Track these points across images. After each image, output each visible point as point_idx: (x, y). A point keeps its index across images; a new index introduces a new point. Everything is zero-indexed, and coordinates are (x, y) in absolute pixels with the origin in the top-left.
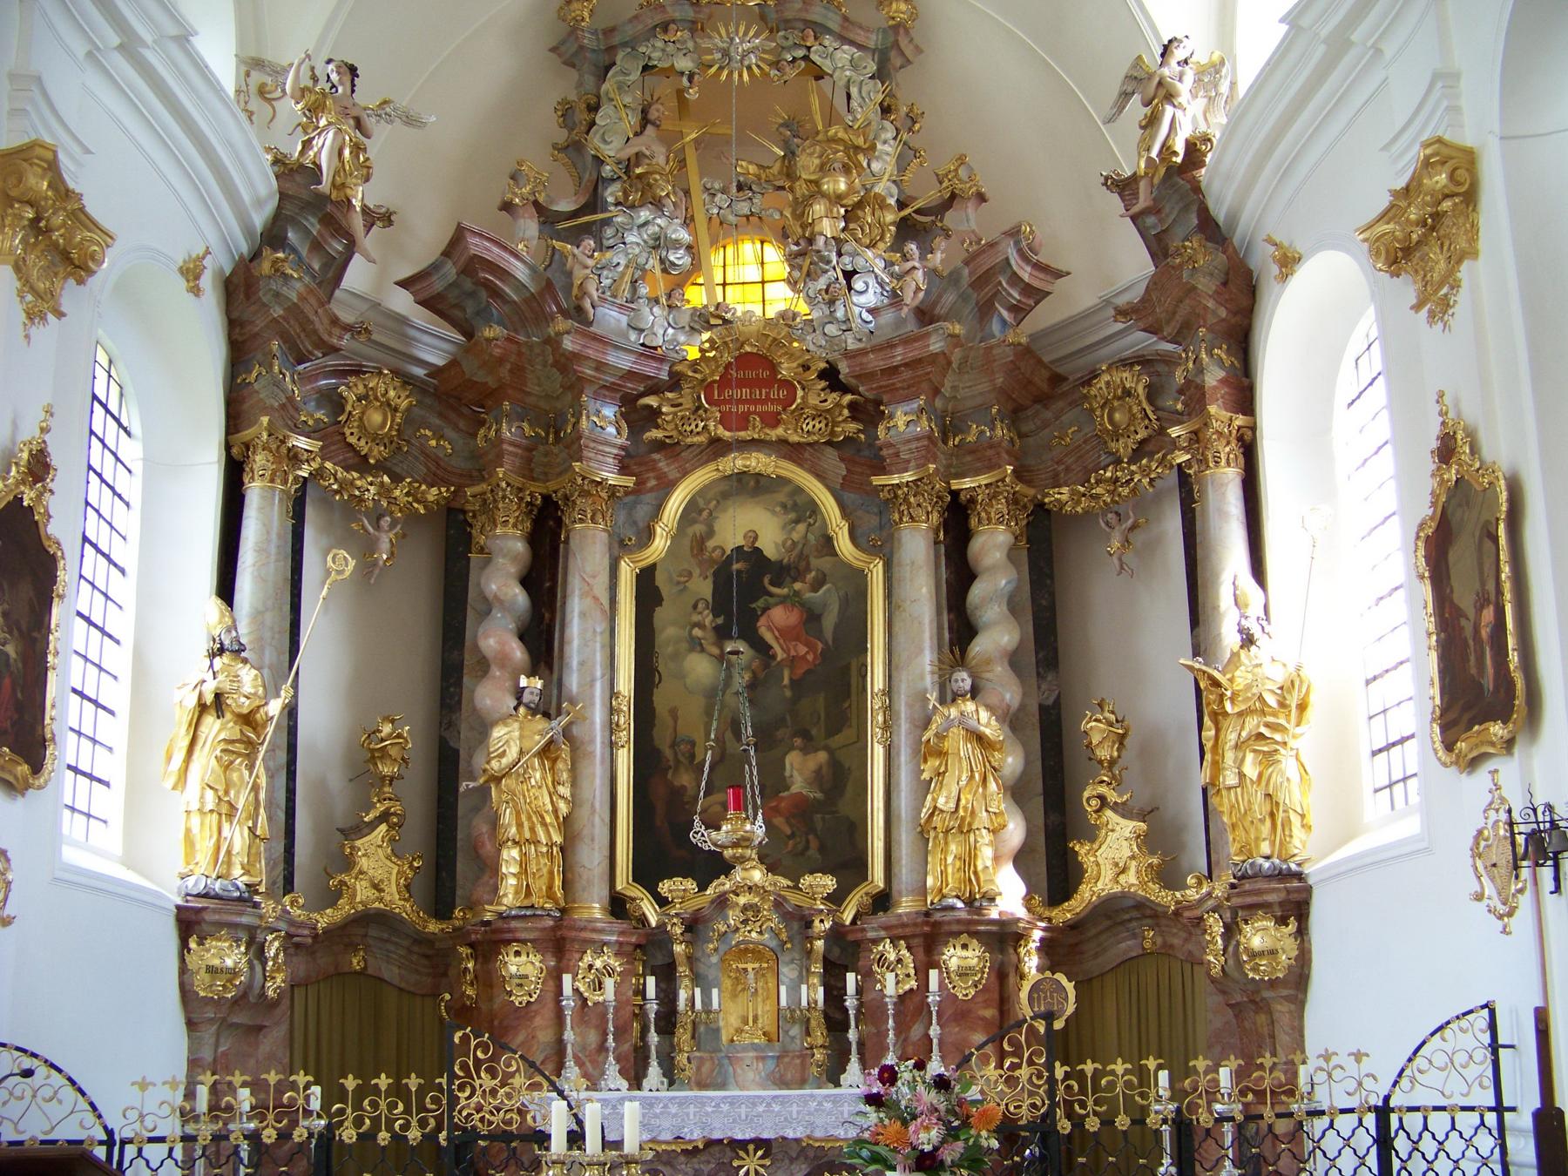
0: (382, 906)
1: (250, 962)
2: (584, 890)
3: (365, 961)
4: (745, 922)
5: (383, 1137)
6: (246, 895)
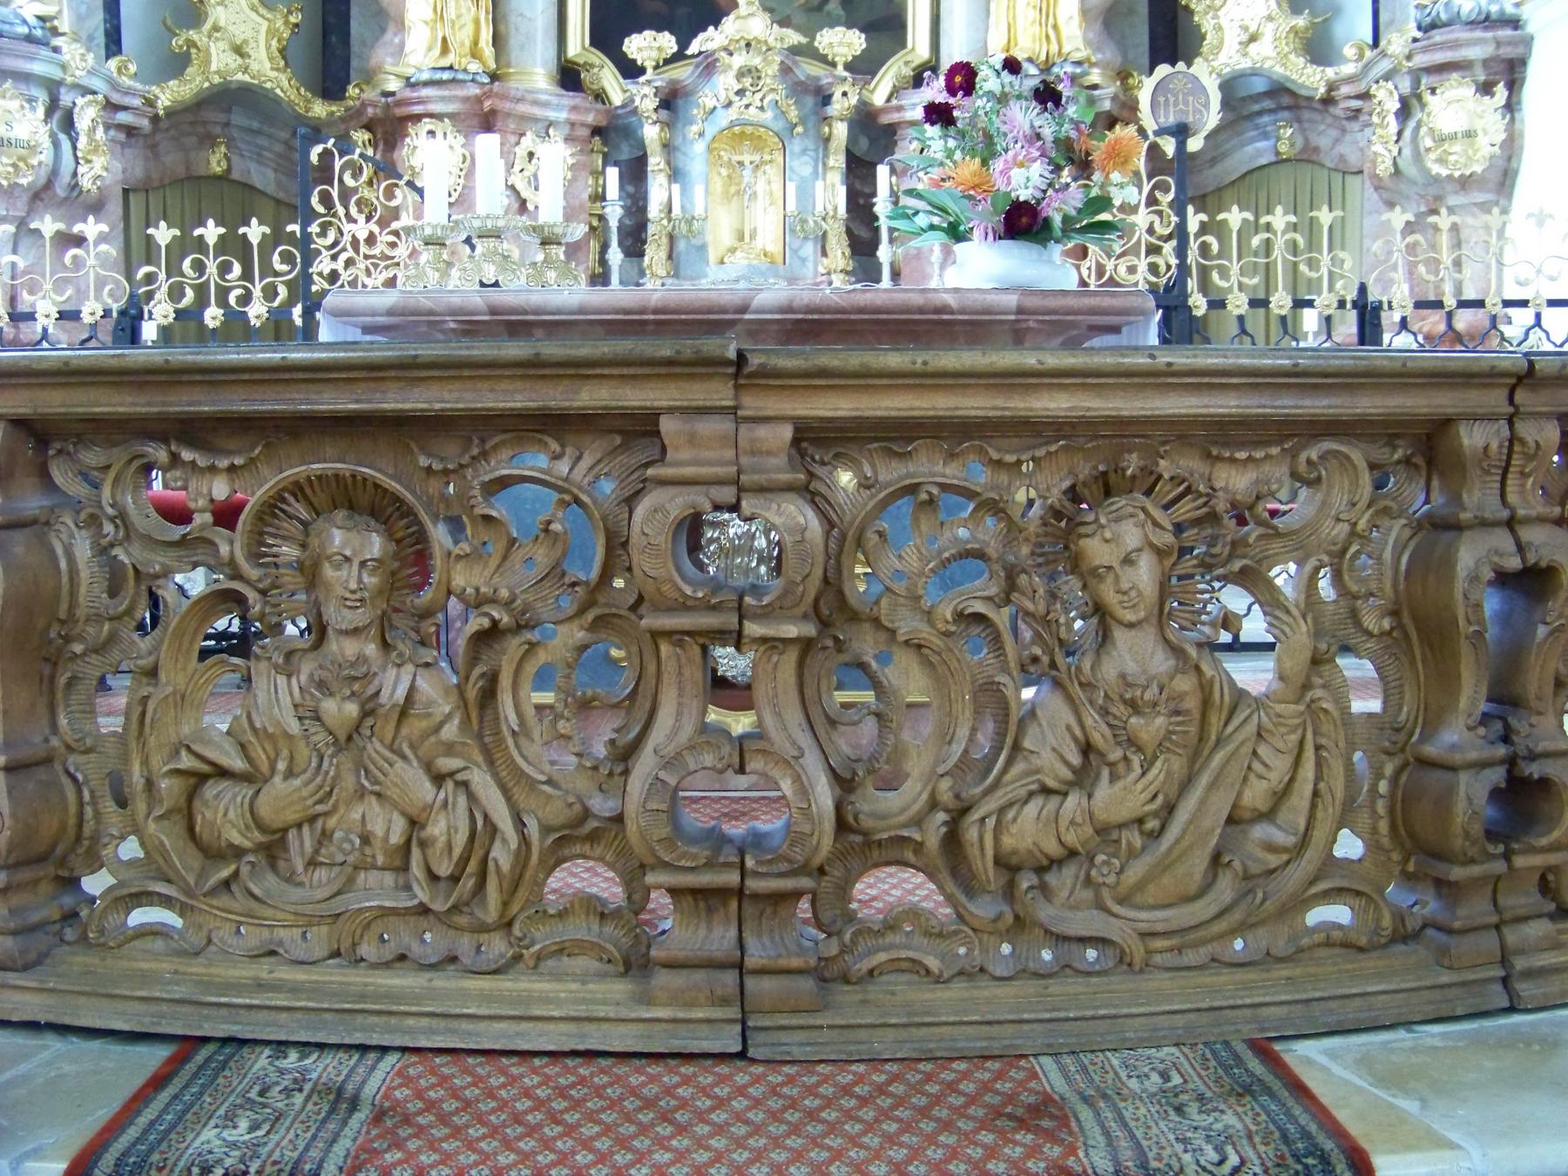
0: (247, 78)
1: (53, 136)
2: (522, 48)
3: (228, 160)
4: (741, 93)
5: (213, 316)
6: (38, 33)
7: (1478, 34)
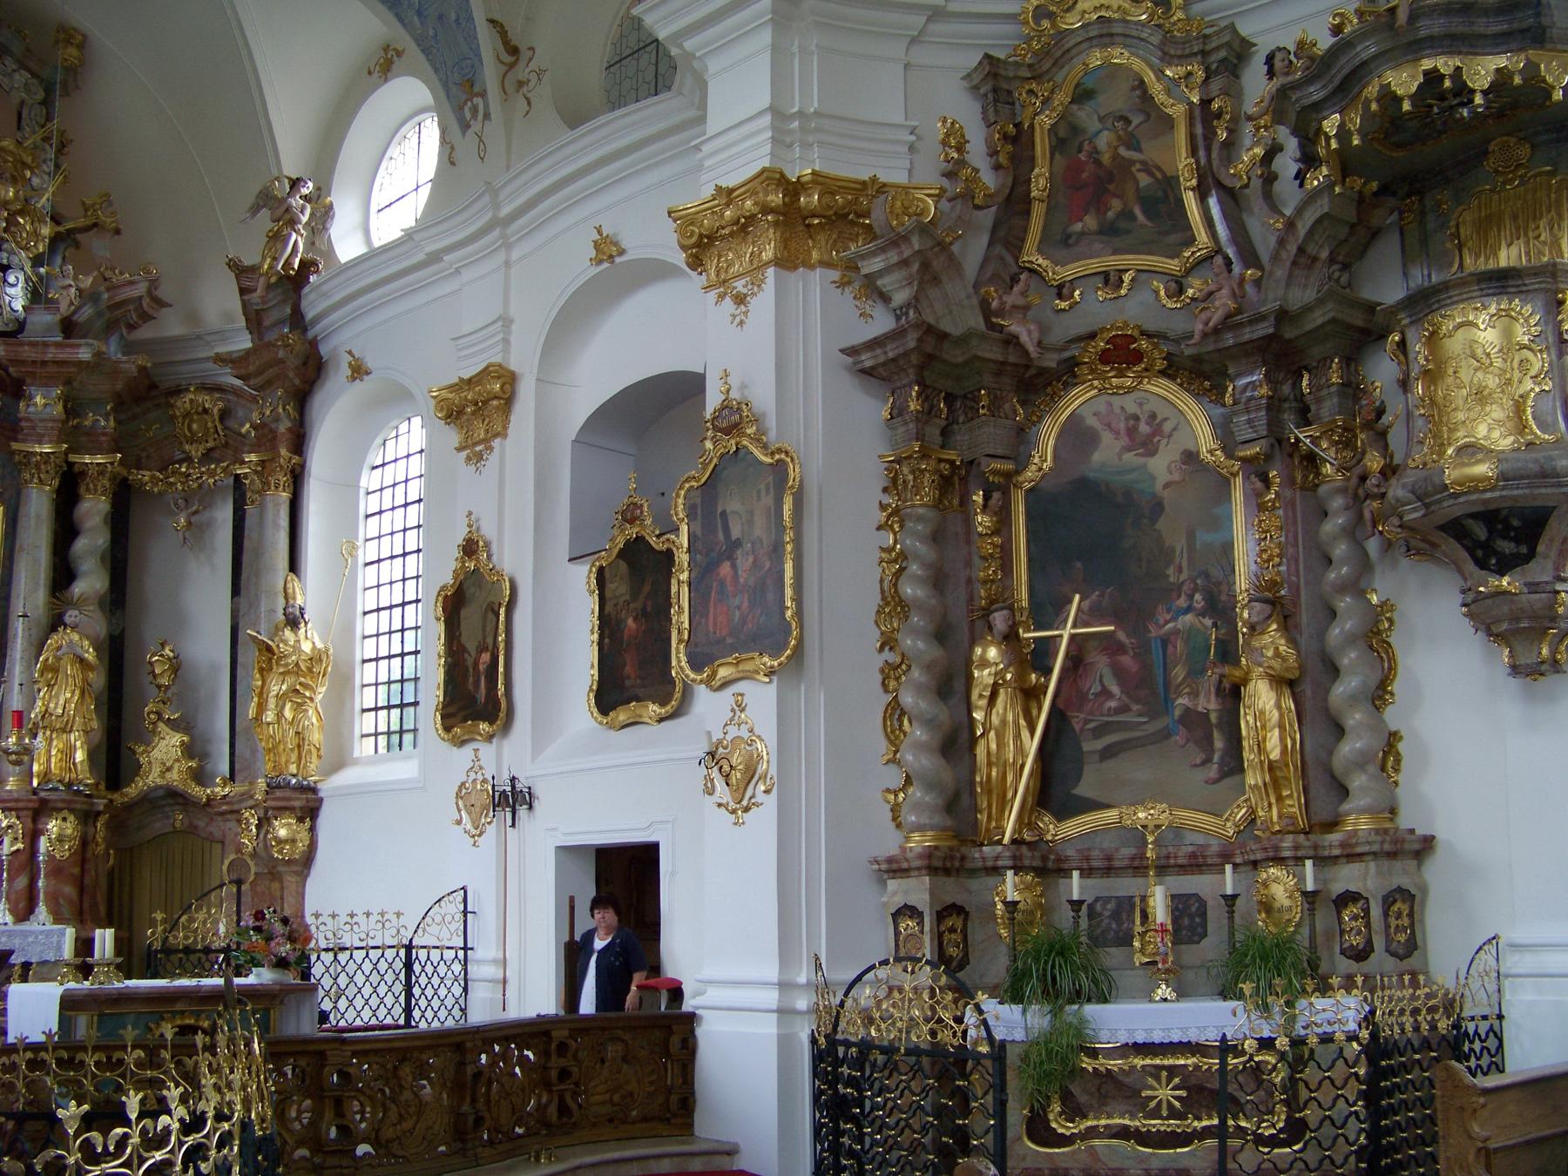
7: (297, 795)
